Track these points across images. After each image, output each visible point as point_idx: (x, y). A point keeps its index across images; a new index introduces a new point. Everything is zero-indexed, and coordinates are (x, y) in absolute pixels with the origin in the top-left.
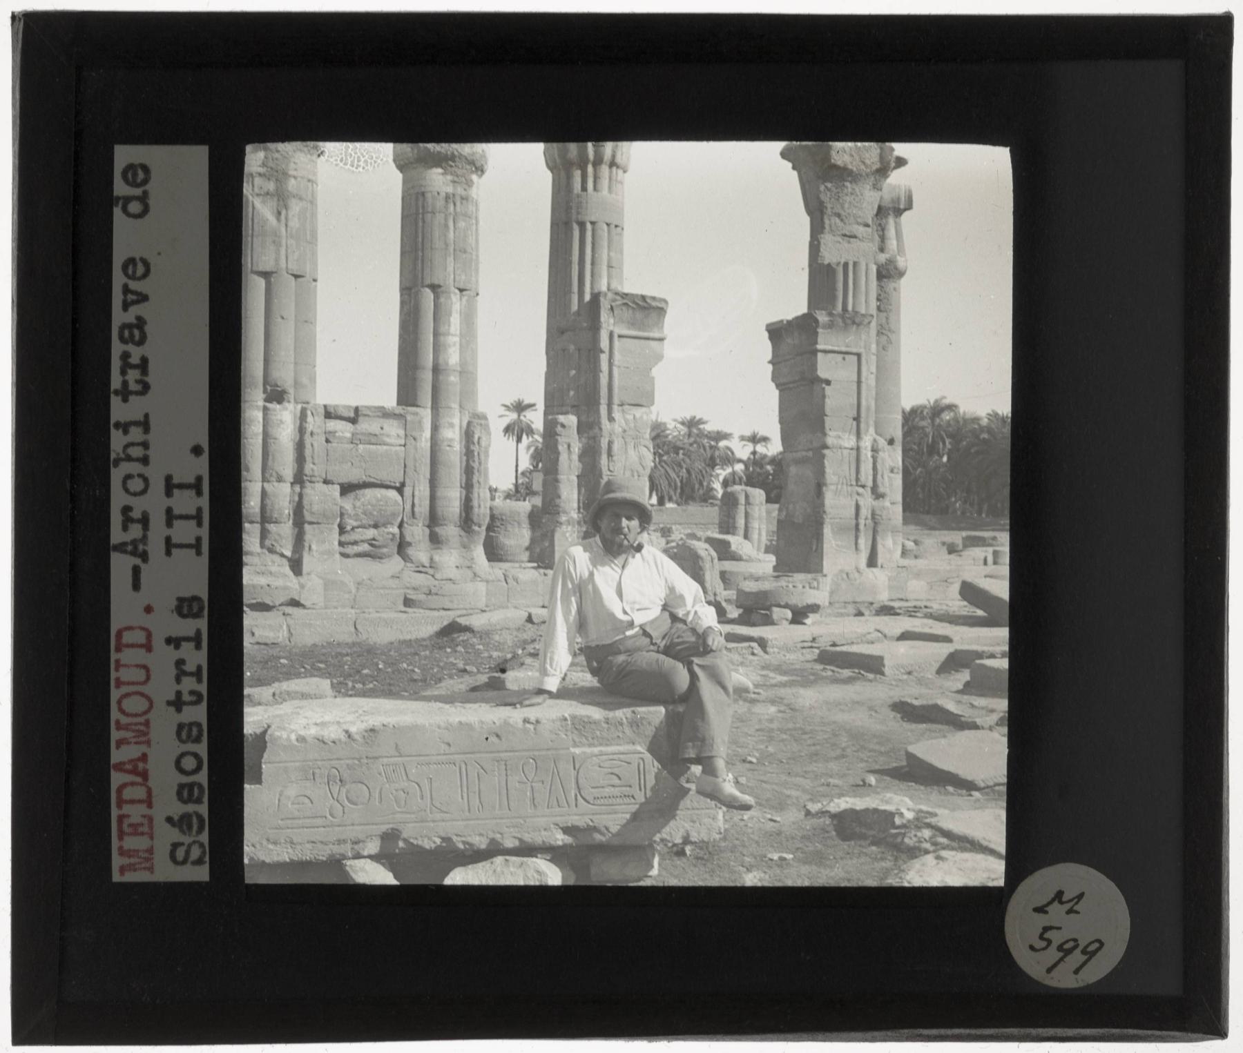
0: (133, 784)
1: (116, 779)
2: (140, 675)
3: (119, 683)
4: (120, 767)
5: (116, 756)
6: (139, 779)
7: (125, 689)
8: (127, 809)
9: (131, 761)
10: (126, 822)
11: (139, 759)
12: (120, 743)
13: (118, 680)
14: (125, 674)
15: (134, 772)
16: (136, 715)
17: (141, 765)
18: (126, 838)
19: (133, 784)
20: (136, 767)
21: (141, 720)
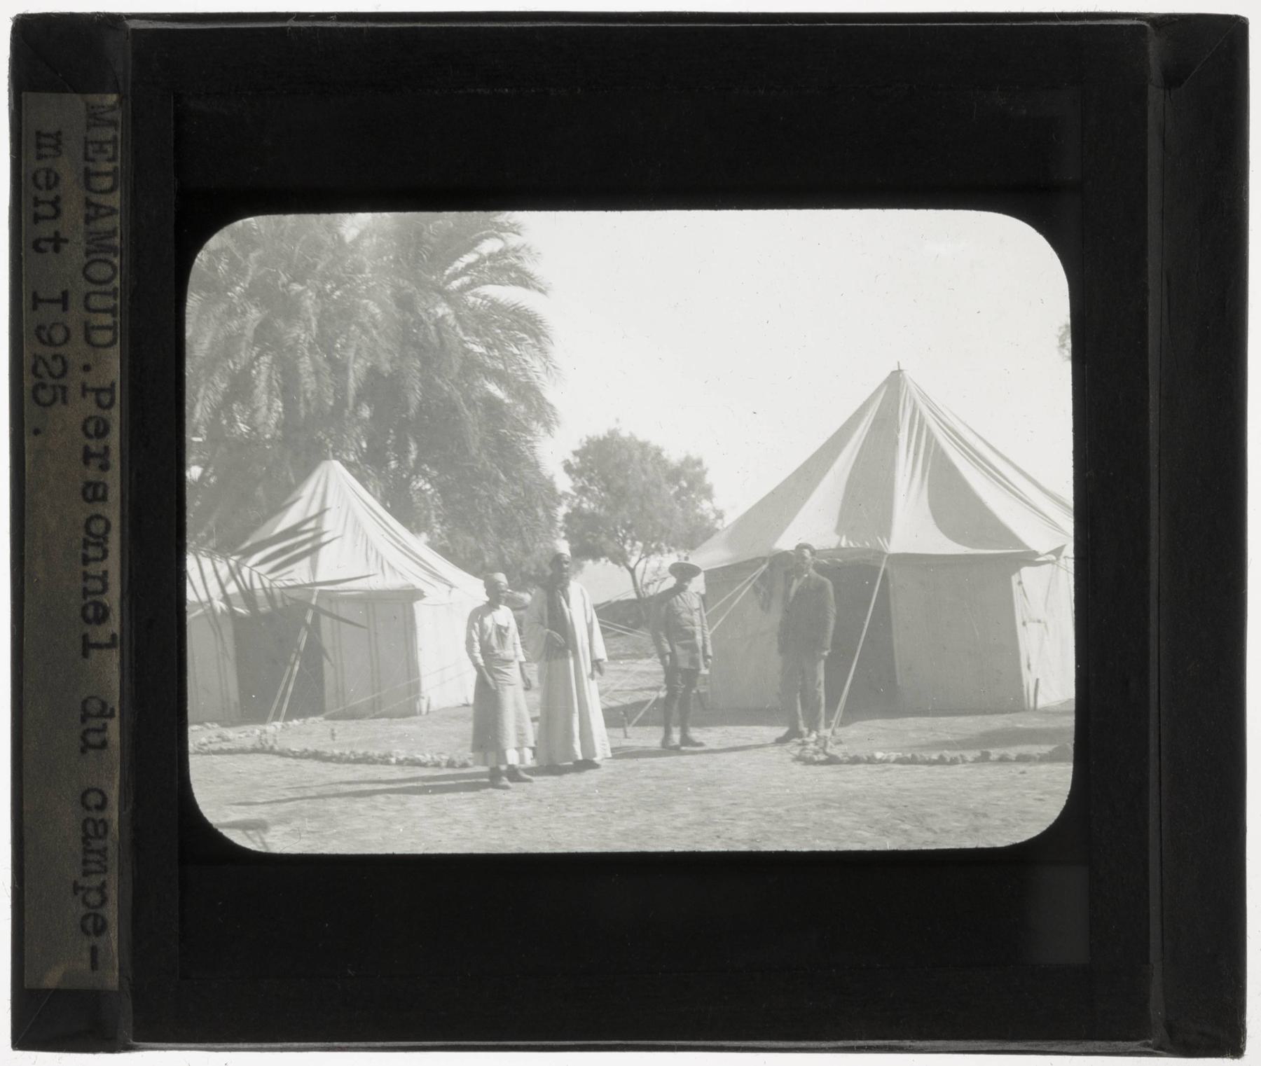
0: (102, 192)
1: (115, 200)
2: (96, 302)
3: (113, 294)
4: (112, 211)
5: (117, 219)
6: (95, 198)
7: (109, 288)
8: (108, 167)
9: (103, 216)
10: (110, 155)
11: (94, 219)
12: (114, 232)
13: (115, 298)
14: (111, 302)
15: (98, 206)
16: (100, 261)
17: (92, 212)
18: (110, 137)
19: (102, 192)
20: (97, 212)
21: (94, 256)
